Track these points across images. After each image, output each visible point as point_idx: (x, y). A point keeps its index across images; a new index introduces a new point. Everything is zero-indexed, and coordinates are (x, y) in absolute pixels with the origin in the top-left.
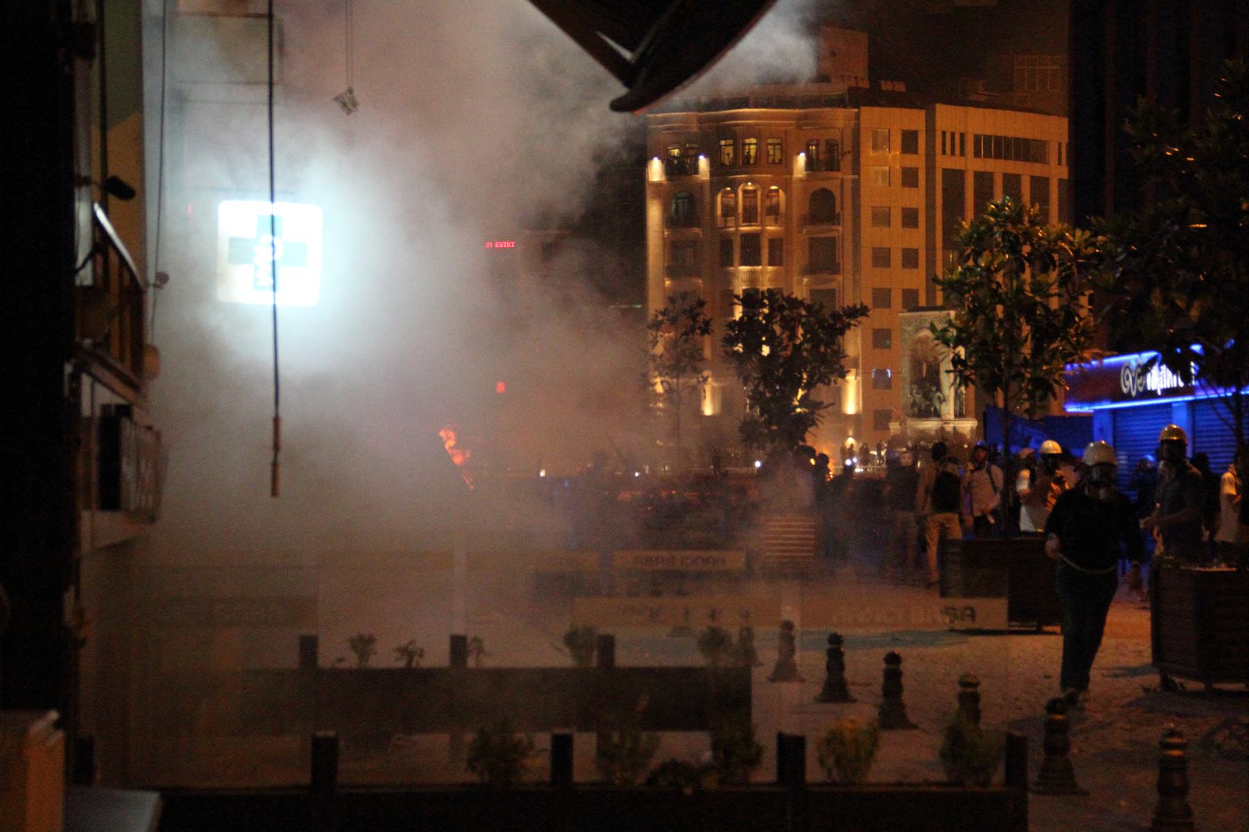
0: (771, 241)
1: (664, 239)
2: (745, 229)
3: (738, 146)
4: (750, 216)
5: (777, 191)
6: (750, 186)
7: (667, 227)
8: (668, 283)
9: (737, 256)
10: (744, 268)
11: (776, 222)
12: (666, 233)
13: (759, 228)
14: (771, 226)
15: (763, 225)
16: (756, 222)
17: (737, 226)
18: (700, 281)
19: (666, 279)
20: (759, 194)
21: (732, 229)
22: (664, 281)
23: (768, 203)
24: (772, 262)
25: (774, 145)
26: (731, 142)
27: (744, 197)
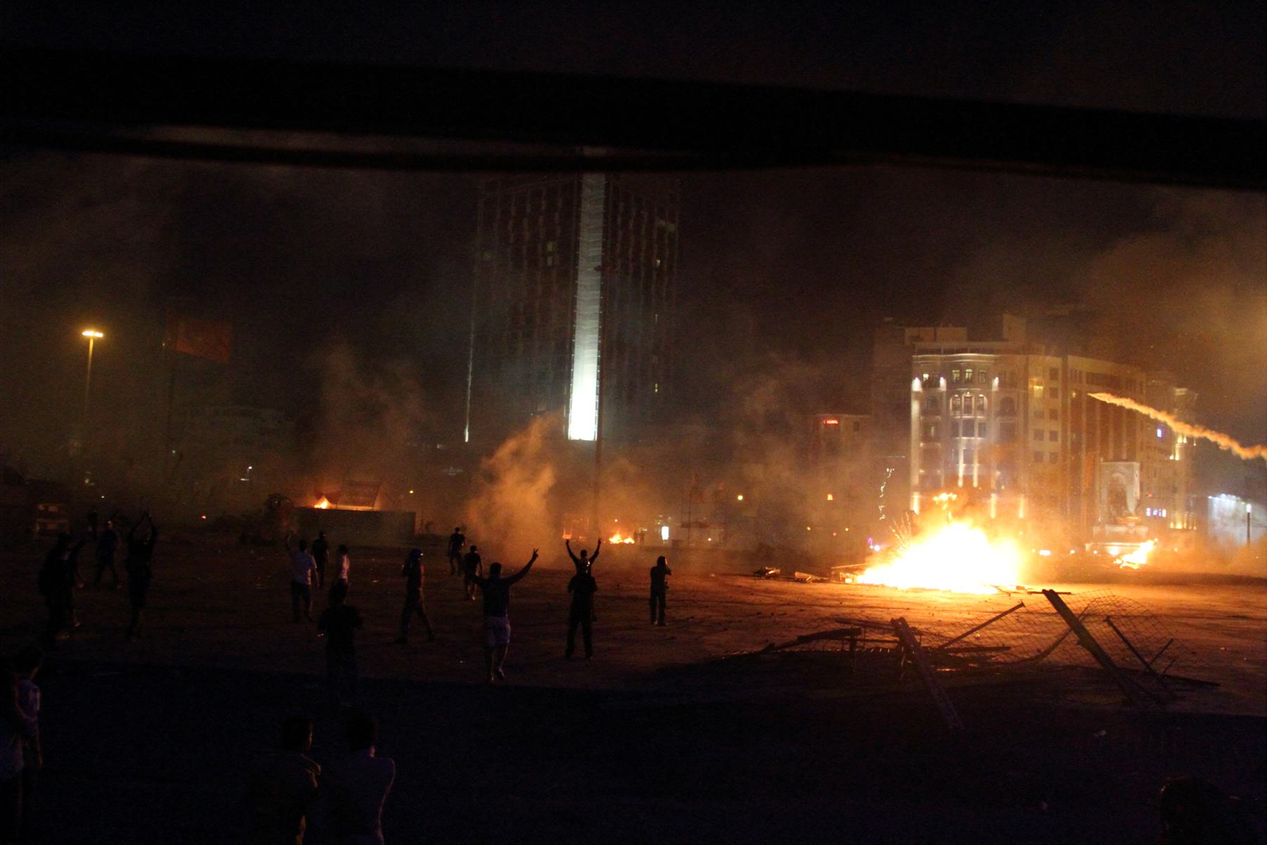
0: (980, 424)
1: (920, 421)
2: (966, 417)
3: (962, 373)
4: (968, 410)
5: (983, 398)
6: (968, 395)
8: (922, 444)
9: (961, 430)
10: (965, 438)
11: (983, 414)
12: (921, 418)
15: (975, 415)
18: (939, 444)
20: (973, 399)
21: (959, 417)
22: (919, 444)
23: (978, 404)
24: (980, 435)
25: (982, 373)
26: (958, 371)
27: (965, 401)
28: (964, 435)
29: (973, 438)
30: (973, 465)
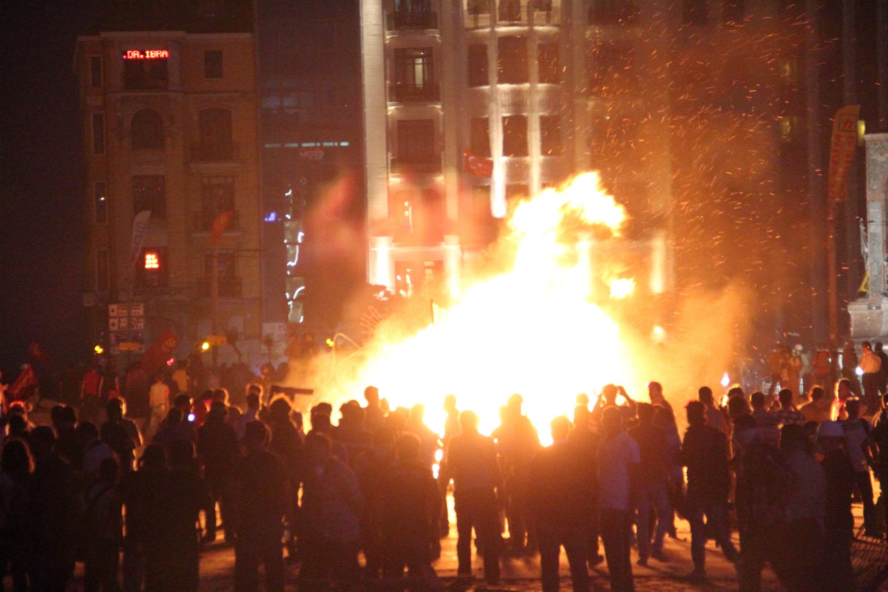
1: (385, 45)
2: (503, 29)
7: (389, 29)
8: (391, 109)
9: (494, 66)
10: (505, 87)
11: (548, 20)
13: (526, 28)
14: (542, 25)
15: (531, 23)
16: (519, 19)
17: (493, 25)
18: (439, 107)
19: (389, 103)
21: (488, 30)
22: (386, 108)
28: (501, 81)
29: (526, 86)
30: (528, 159)
